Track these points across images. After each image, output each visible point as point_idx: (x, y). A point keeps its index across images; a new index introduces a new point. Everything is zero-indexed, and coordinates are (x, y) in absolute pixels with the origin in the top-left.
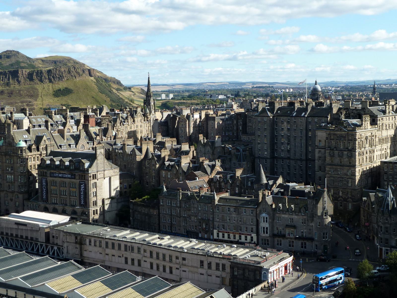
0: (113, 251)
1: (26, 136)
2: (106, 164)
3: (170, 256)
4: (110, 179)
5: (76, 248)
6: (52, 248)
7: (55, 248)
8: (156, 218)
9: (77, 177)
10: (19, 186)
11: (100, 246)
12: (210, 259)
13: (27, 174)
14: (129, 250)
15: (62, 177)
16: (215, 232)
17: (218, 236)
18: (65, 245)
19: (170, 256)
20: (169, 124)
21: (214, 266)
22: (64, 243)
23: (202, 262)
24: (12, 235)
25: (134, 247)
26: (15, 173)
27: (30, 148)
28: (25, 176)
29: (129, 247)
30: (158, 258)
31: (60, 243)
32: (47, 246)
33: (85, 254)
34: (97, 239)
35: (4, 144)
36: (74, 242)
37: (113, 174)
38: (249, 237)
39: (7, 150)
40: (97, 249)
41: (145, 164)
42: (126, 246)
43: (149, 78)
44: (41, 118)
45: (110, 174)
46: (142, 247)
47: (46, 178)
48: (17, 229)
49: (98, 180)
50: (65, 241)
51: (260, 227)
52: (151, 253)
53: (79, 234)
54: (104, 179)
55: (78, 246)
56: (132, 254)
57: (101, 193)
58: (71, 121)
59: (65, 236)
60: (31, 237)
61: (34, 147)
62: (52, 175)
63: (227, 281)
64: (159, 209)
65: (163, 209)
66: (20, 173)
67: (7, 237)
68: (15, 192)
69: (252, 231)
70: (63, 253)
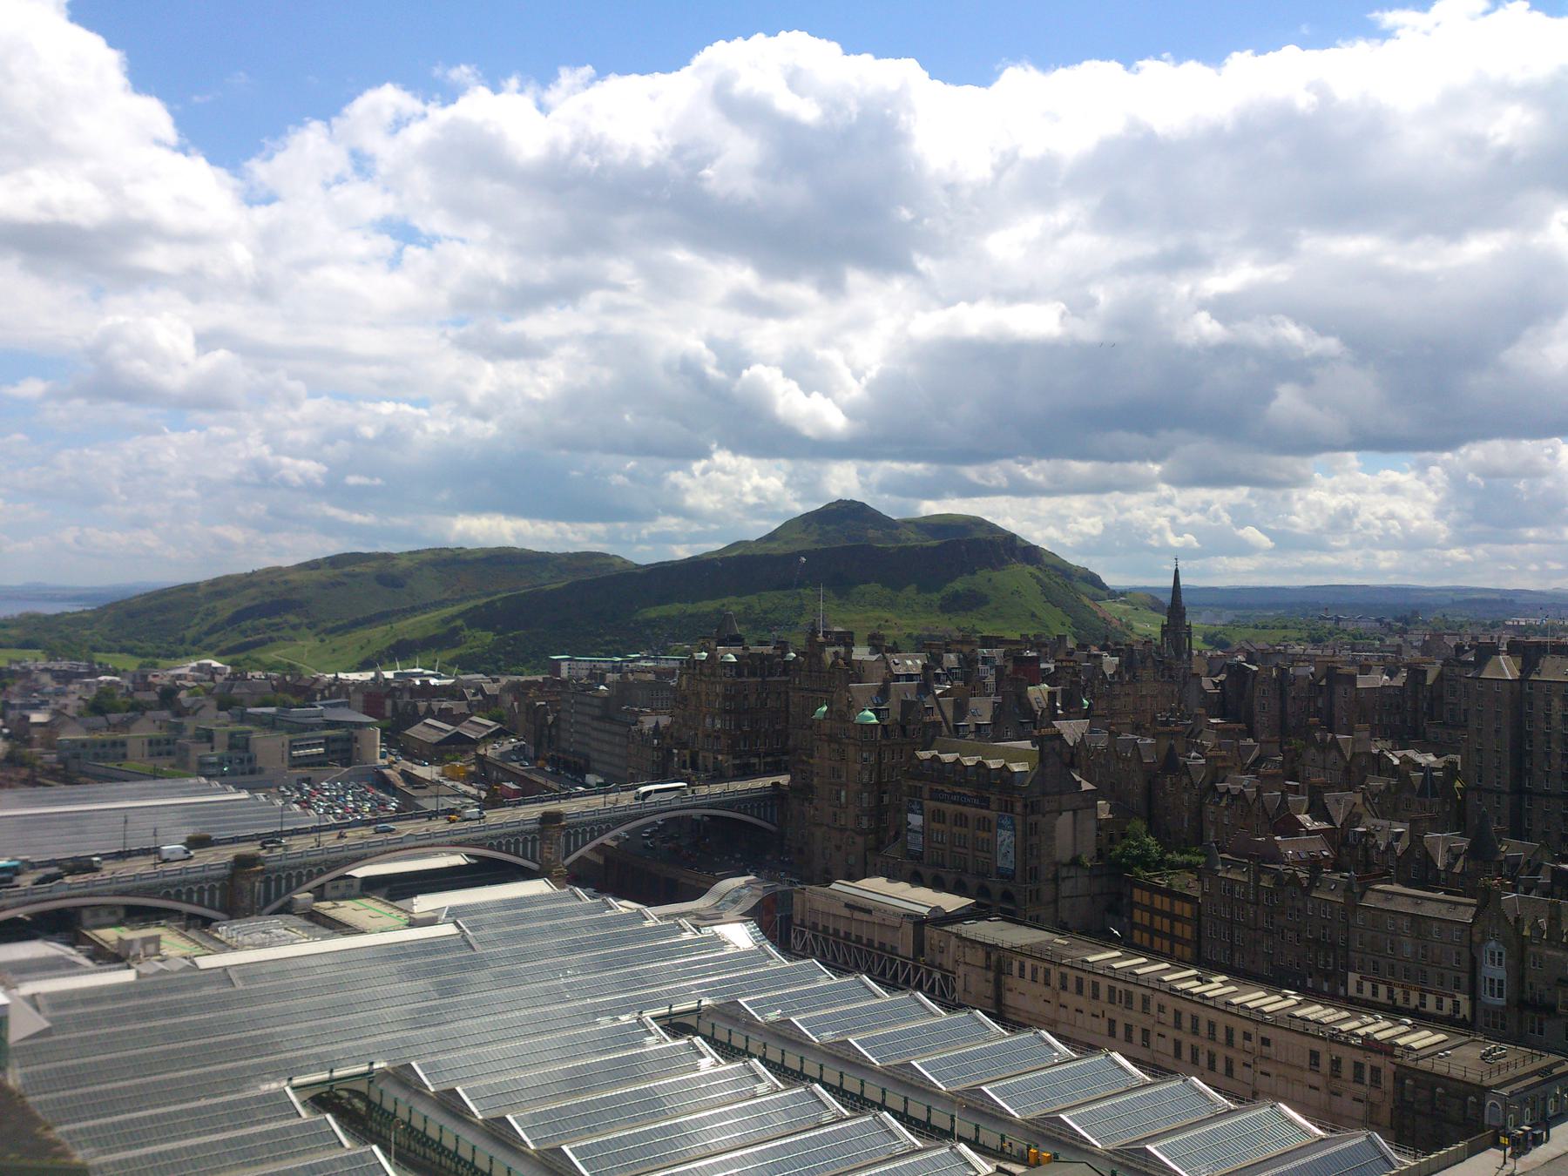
3: (1229, 1032)
4: (1075, 812)
6: (929, 974)
7: (937, 975)
9: (993, 806)
11: (1047, 984)
12: (1337, 1050)
16: (1353, 978)
17: (1360, 990)
18: (961, 970)
19: (1229, 1032)
21: (1347, 1071)
23: (1314, 1055)
24: (836, 932)
30: (1195, 1030)
31: (948, 963)
32: (917, 969)
33: (1009, 999)
34: (1039, 964)
38: (1447, 1002)
40: (1039, 989)
42: (1112, 989)
48: (851, 919)
51: (1480, 979)
52: (1178, 1014)
53: (995, 947)
56: (1127, 1012)
63: (1385, 1115)
69: (1457, 987)
70: (954, 990)
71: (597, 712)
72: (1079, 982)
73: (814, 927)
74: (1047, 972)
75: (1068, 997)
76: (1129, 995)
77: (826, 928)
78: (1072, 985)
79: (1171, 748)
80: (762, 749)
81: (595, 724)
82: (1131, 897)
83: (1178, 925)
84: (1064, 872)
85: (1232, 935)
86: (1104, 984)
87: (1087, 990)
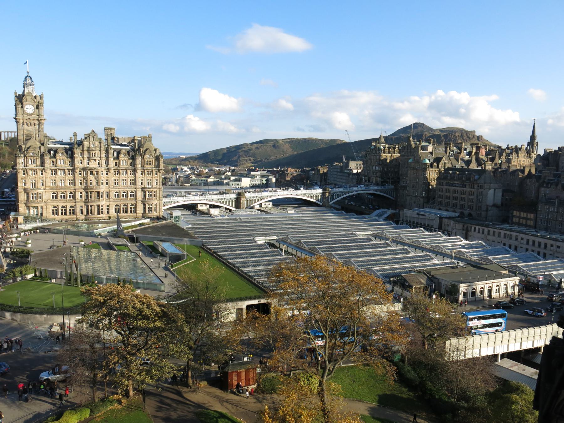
0: (494, 237)
4: (495, 190)
9: (467, 187)
11: (483, 233)
18: (454, 231)
20: (550, 159)
27: (431, 166)
31: (450, 229)
42: (505, 234)
44: (441, 147)
48: (418, 218)
56: (510, 241)
61: (435, 164)
64: (537, 214)
71: (339, 170)
73: (407, 221)
74: (483, 230)
76: (511, 235)
77: (410, 221)
79: (530, 170)
80: (391, 177)
81: (339, 174)
82: (513, 213)
83: (529, 221)
84: (490, 208)
85: (547, 223)
87: (497, 235)
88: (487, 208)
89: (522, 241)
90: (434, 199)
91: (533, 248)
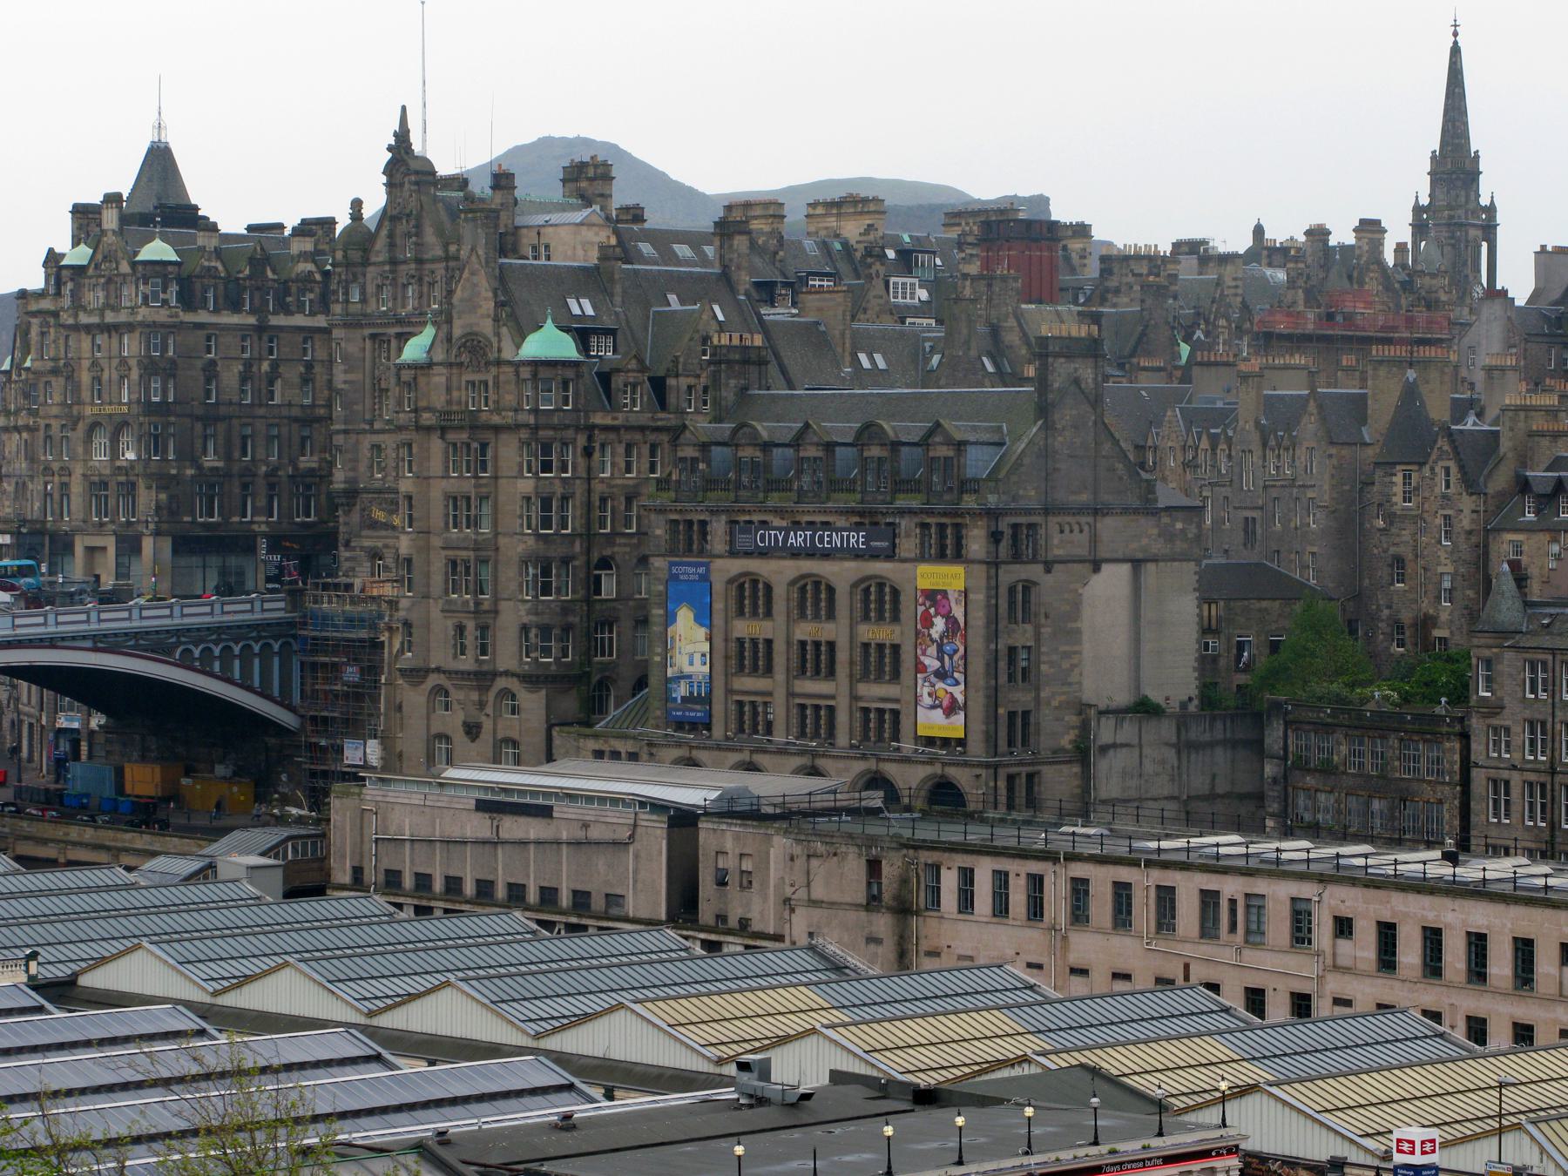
1: (586, 303)
2: (1112, 470)
3: (1524, 950)
5: (872, 940)
8: (1440, 802)
10: (525, 629)
11: (1036, 909)
13: (577, 547)
14: (1233, 927)
15: (811, 553)
19: (1524, 950)
22: (792, 910)
25: (1270, 905)
26: (502, 541)
28: (565, 561)
29: (1233, 902)
30: (1433, 964)
35: (439, 356)
36: (861, 898)
37: (1158, 547)
39: (455, 394)
41: (1388, 498)
42: (1209, 899)
43: (1455, 51)
45: (1135, 545)
46: (1325, 905)
47: (707, 565)
48: (494, 844)
49: (1048, 571)
50: (802, 894)
52: (1387, 934)
54: (1096, 568)
55: (883, 924)
56: (1251, 957)
57: (1065, 665)
58: (900, 280)
59: (800, 863)
60: (575, 893)
62: (743, 541)
65: (1496, 730)
66: (531, 541)
67: (424, 903)
68: (495, 674)
72: (1122, 892)
73: (392, 881)
74: (1036, 882)
75: (1095, 947)
76: (1255, 903)
78: (1101, 906)
79: (1410, 393)
84: (1105, 732)
86: (1188, 887)
87: (1144, 910)
88: (1085, 727)
89: (1344, 945)
90: (641, 683)
91: (1431, 996)
